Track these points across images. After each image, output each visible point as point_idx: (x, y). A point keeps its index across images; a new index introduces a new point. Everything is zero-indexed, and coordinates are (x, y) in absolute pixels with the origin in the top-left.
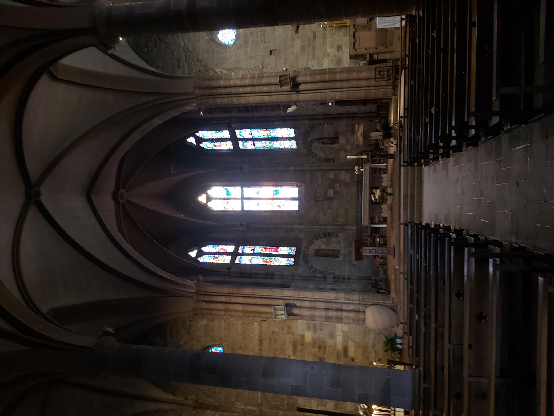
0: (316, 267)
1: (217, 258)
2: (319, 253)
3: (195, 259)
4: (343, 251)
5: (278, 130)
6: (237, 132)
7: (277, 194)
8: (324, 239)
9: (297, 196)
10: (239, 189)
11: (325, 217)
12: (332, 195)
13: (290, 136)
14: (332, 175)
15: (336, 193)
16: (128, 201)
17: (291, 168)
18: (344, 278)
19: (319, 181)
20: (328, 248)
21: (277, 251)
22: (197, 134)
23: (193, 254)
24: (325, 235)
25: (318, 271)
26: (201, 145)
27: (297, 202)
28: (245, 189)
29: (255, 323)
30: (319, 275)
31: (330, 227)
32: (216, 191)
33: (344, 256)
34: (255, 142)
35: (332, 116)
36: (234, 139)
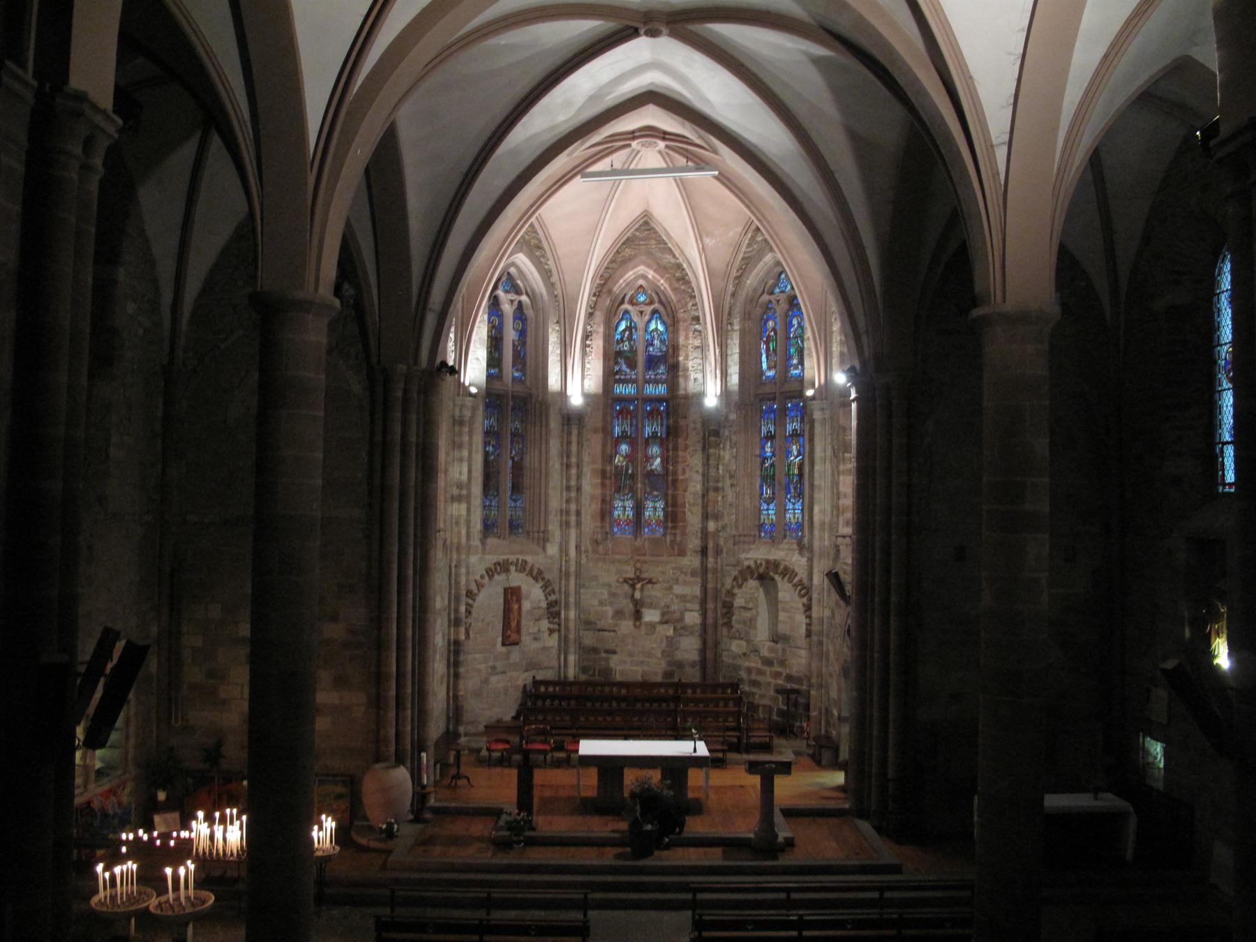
0: (481, 598)
2: (512, 595)
8: (544, 605)
14: (693, 618)
15: (652, 626)
18: (457, 664)
19: (678, 589)
20: (523, 614)
24: (551, 605)
25: (470, 601)
30: (463, 609)
31: (572, 614)
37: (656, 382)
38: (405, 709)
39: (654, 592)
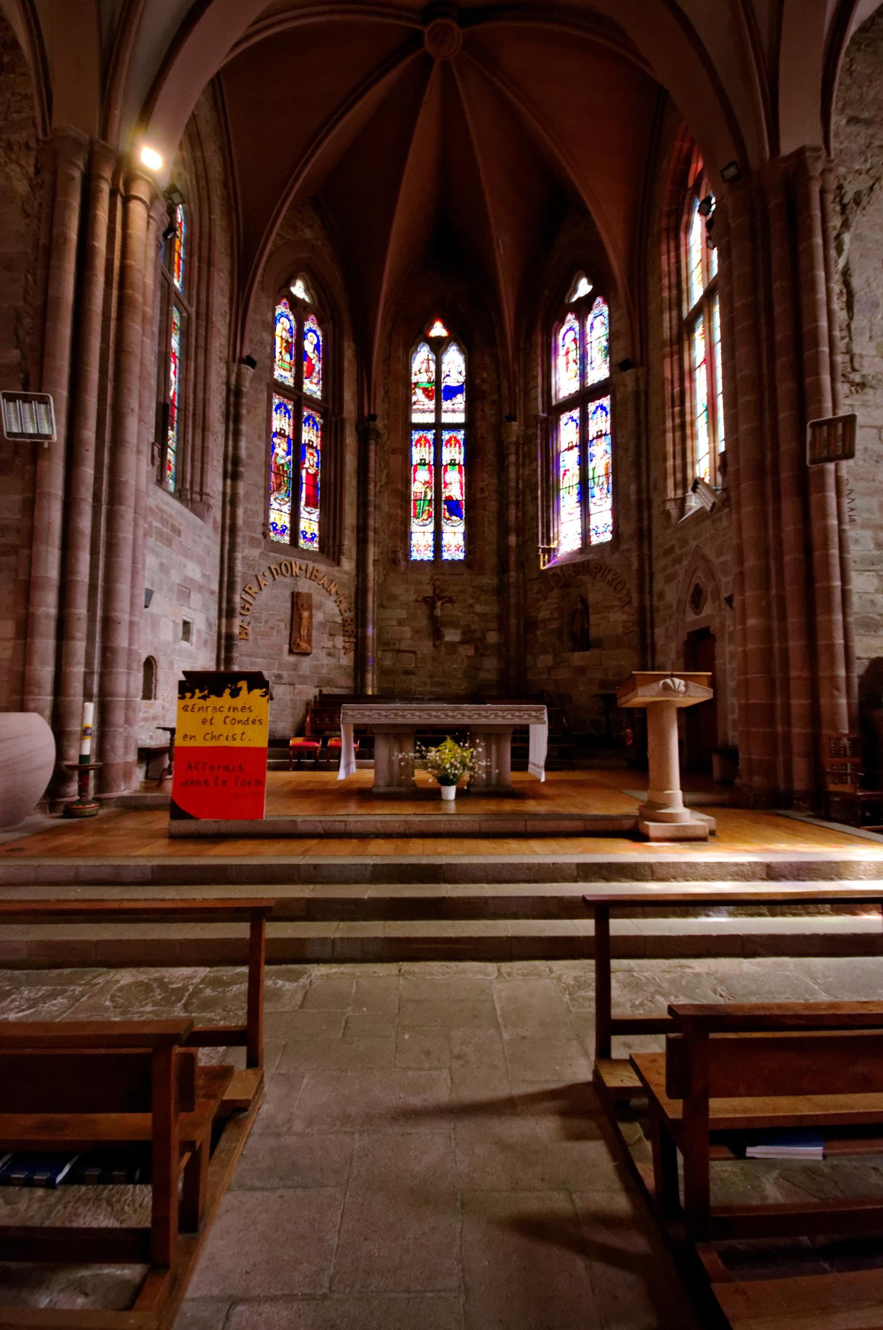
1: (288, 350)
3: (283, 292)
4: (306, 664)
5: (608, 503)
6: (606, 401)
7: (449, 510)
8: (339, 620)
9: (446, 556)
10: (460, 418)
11: (394, 622)
12: (447, 639)
13: (592, 533)
14: (492, 637)
15: (453, 646)
16: (427, 61)
17: (513, 540)
19: (479, 609)
21: (307, 505)
22: (599, 300)
23: (299, 290)
26: (570, 317)
27: (429, 555)
28: (461, 435)
29: (17, 353)
30: (237, 599)
32: (455, 364)
33: (295, 667)
34: (576, 450)
35: (649, 630)
36: (584, 397)
37: (454, 411)
38: (72, 638)
39: (455, 611)
